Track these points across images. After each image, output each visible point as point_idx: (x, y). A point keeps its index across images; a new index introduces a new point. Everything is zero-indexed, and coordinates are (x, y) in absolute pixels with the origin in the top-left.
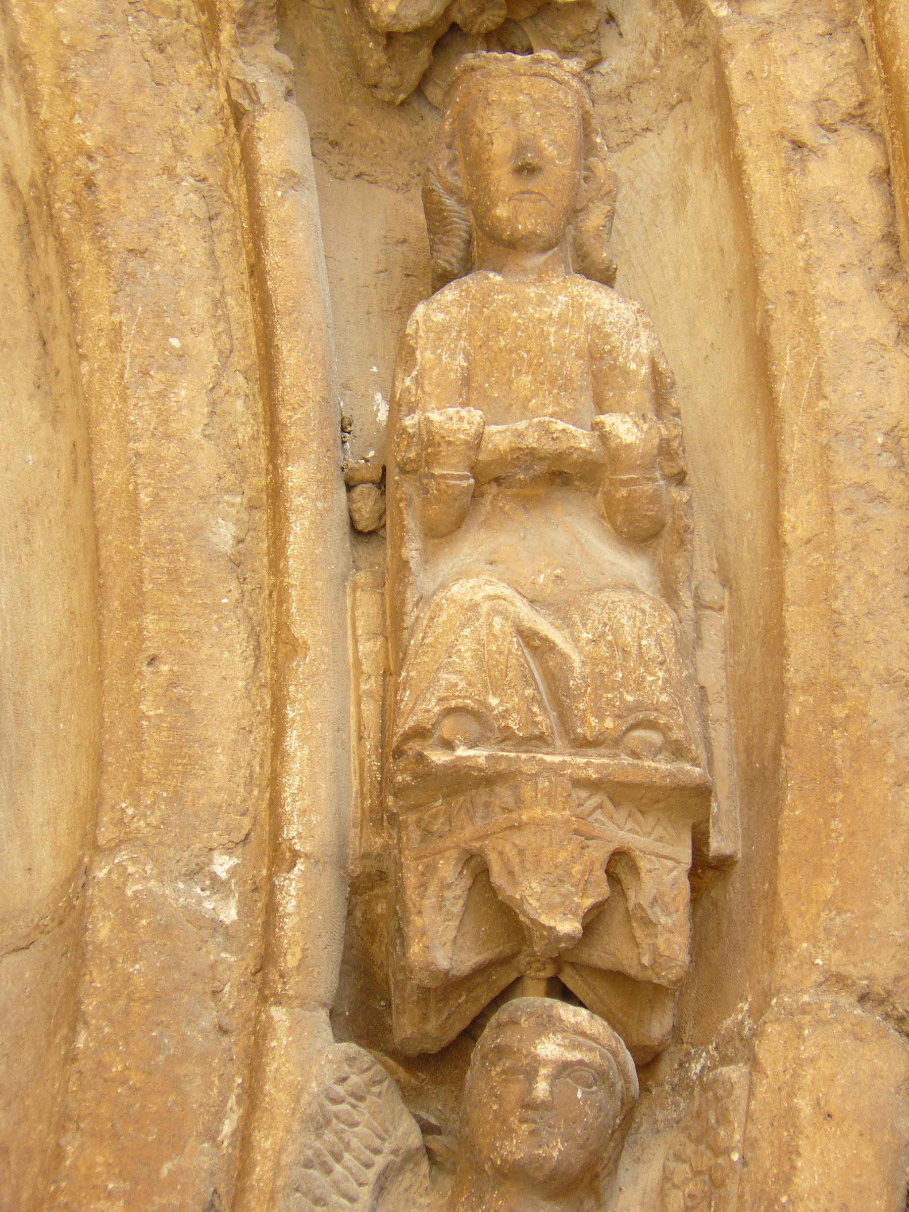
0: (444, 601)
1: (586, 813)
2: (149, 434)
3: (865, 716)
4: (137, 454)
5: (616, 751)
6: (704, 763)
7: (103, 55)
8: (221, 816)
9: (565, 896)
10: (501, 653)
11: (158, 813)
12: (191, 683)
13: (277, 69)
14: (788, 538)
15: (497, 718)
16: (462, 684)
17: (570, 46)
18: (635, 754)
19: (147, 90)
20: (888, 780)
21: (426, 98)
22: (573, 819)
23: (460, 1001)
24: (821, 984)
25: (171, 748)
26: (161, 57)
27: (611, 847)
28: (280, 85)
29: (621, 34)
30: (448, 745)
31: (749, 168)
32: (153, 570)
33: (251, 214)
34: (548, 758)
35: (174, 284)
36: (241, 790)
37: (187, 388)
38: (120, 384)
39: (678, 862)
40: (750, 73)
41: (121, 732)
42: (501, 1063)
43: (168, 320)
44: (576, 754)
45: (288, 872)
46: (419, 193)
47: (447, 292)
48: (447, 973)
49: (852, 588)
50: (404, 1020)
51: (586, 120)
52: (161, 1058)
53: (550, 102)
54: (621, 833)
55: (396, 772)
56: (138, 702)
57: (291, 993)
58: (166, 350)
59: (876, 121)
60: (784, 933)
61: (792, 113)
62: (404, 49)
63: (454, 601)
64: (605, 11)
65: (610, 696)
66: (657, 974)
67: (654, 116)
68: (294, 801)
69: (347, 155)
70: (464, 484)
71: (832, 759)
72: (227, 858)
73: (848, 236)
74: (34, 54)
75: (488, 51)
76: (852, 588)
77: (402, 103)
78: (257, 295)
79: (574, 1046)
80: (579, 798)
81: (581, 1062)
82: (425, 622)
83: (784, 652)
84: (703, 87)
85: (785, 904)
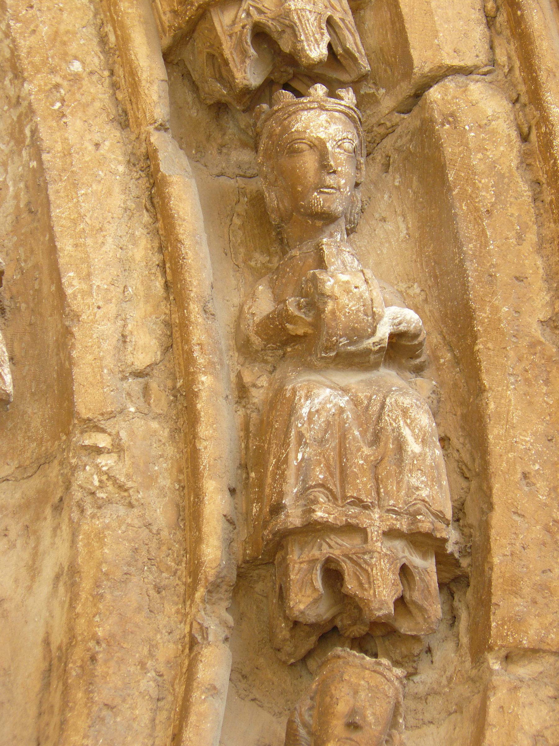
7: (123, 585)
13: (224, 623)
17: (400, 659)
19: (143, 613)
21: (306, 665)
26: (158, 596)
28: (223, 633)
29: (432, 662)
35: (125, 732)
40: (502, 707)
46: (286, 721)
51: (397, 706)
53: (378, 690)
61: (519, 738)
62: (302, 633)
67: (438, 716)
74: (83, 572)
75: (351, 649)
77: (292, 664)
84: (472, 707)
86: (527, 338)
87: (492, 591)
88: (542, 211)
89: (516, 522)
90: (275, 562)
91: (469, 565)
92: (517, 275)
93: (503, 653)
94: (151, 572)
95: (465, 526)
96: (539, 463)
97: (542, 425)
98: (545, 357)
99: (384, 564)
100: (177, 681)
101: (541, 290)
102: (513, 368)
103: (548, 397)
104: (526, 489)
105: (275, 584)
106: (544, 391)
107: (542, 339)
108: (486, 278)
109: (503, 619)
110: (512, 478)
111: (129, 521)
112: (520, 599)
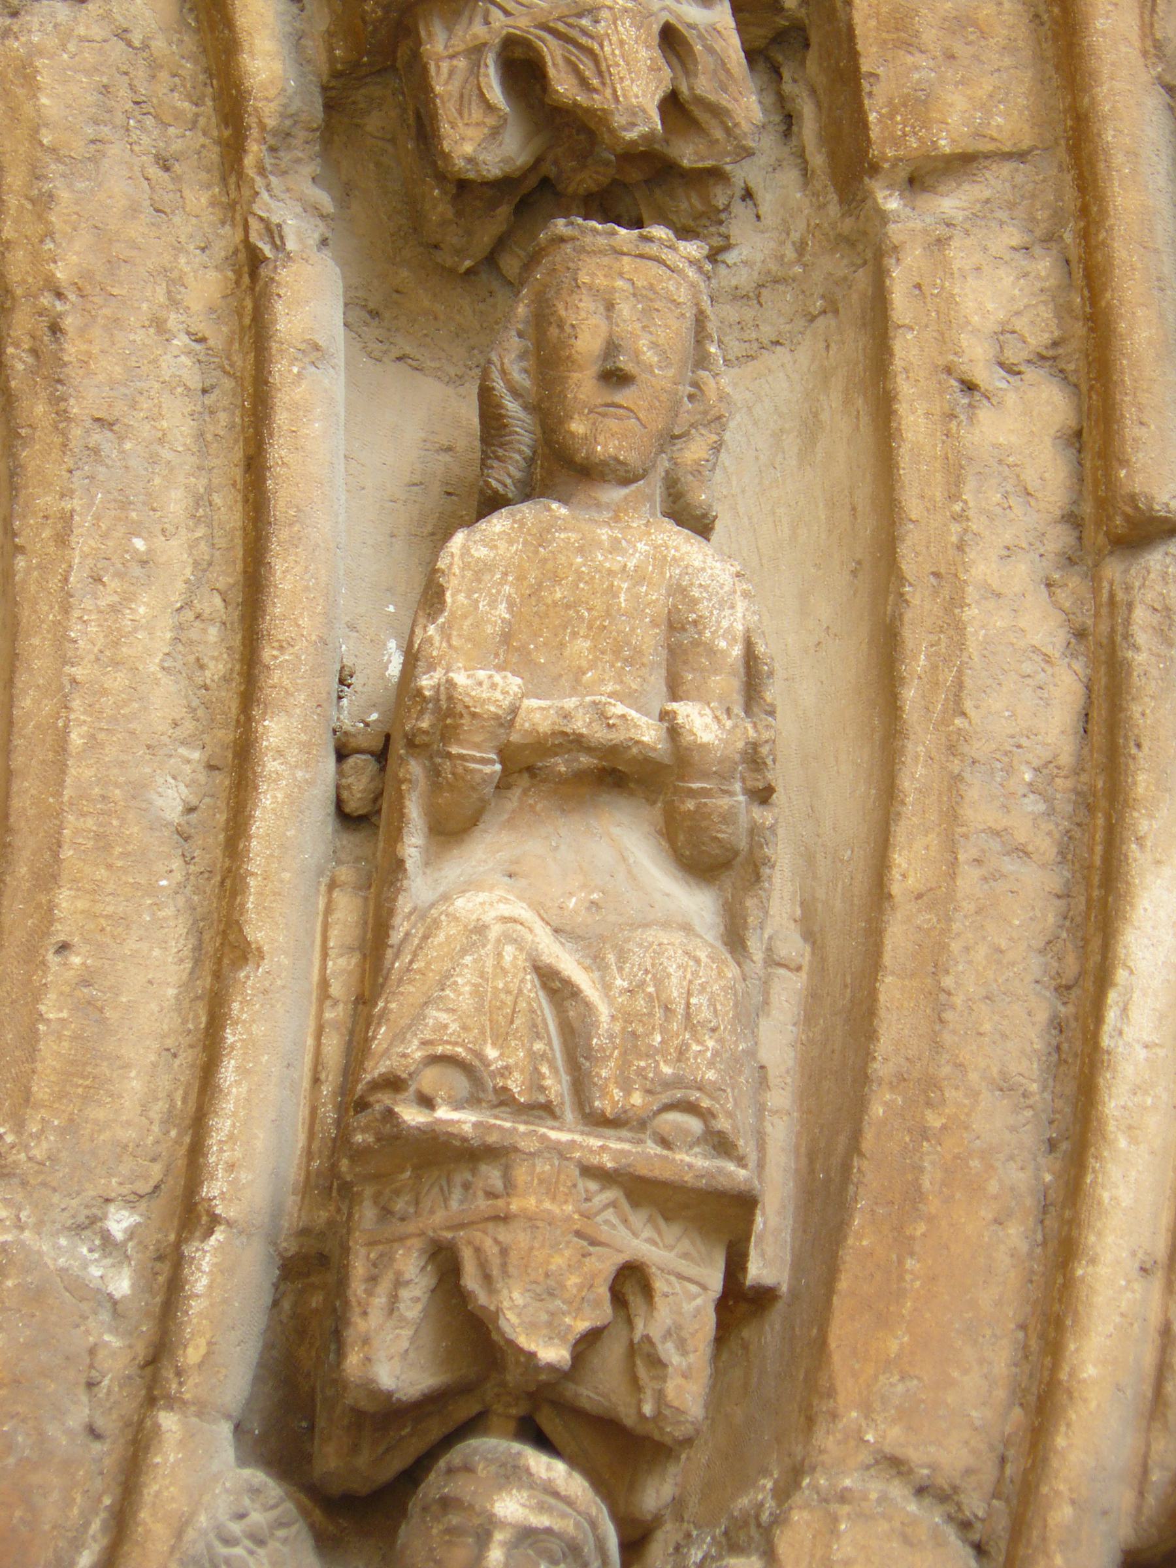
0: (443, 917)
1: (594, 1210)
2: (92, 657)
3: (966, 1128)
4: (74, 681)
5: (642, 1136)
6: (752, 1164)
8: (125, 1158)
9: (552, 1314)
10: (508, 992)
11: (45, 1145)
12: (107, 984)
13: (314, 210)
14: (896, 889)
15: (493, 1075)
16: (454, 1027)
17: (692, 224)
18: (665, 1143)
19: (142, 216)
20: (987, 1214)
21: (498, 268)
22: (576, 1216)
23: (403, 1433)
24: (868, 1467)
25: (73, 1063)
26: (166, 175)
27: (620, 1259)
28: (314, 231)
29: (758, 217)
30: (427, 1102)
31: (902, 408)
32: (77, 832)
33: (256, 391)
34: (554, 1135)
36: (156, 1128)
37: (147, 605)
38: (62, 589)
39: (704, 1288)
41: (10, 1036)
42: (445, 1519)
43: (134, 515)
44: (589, 1134)
45: (202, 1242)
47: (495, 521)
48: (389, 1394)
49: (970, 962)
50: (330, 1449)
51: (700, 320)
52: (11, 1460)
54: (635, 1242)
55: (355, 1130)
56: (37, 1000)
57: (187, 1396)
58: (127, 552)
59: (1072, 367)
60: (829, 1396)
61: (965, 344)
62: (478, 203)
63: (456, 919)
64: (743, 185)
65: (642, 1064)
66: (661, 1429)
67: (788, 327)
68: (221, 1151)
69: (389, 330)
70: (487, 769)
71: (917, 1179)
72: (126, 1213)
73: (1018, 510)
76: (970, 962)
77: (469, 272)
78: (252, 496)
79: (541, 1508)
80: (587, 1191)
81: (548, 1531)
82: (416, 941)
83: (871, 1035)
84: (855, 297)
85: (836, 1358)
87: (859, 47)
90: (399, 65)
93: (903, 174)
94: (143, 129)
99: (626, 30)
100: (236, 346)
105: (404, 110)
109: (890, 102)
111: (81, 31)
112: (918, 55)
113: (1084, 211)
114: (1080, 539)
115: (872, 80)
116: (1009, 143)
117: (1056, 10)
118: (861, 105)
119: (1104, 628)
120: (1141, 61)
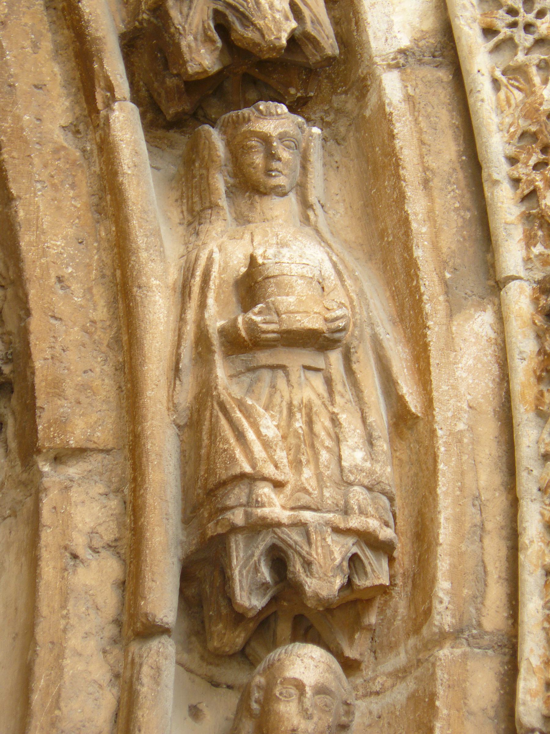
31: (43, 564)
59: (123, 551)
61: (74, 537)
73: (93, 616)
84: (25, 510)
86: (50, 145)
87: (36, 394)
88: (55, 19)
89: (54, 325)
91: (12, 372)
92: (36, 83)
93: (52, 455)
95: (5, 334)
96: (72, 266)
97: (72, 228)
98: (70, 162)
101: (59, 96)
102: (39, 175)
103: (75, 201)
104: (61, 292)
106: (71, 195)
107: (65, 144)
108: (7, 88)
109: (49, 421)
110: (46, 283)
112: (63, 400)
113: (134, 480)
114: (120, 632)
115: (41, 410)
116: (102, 445)
117: (129, 385)
118: (35, 421)
119: (128, 674)
120: (166, 412)
